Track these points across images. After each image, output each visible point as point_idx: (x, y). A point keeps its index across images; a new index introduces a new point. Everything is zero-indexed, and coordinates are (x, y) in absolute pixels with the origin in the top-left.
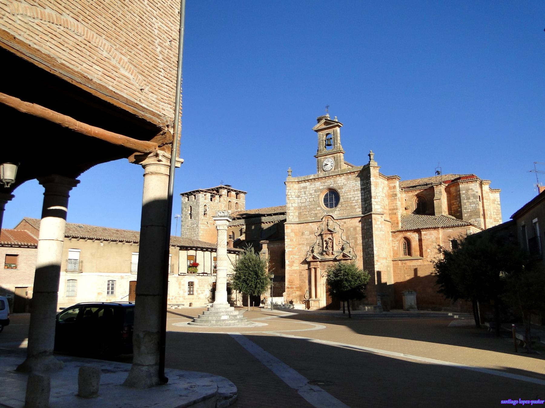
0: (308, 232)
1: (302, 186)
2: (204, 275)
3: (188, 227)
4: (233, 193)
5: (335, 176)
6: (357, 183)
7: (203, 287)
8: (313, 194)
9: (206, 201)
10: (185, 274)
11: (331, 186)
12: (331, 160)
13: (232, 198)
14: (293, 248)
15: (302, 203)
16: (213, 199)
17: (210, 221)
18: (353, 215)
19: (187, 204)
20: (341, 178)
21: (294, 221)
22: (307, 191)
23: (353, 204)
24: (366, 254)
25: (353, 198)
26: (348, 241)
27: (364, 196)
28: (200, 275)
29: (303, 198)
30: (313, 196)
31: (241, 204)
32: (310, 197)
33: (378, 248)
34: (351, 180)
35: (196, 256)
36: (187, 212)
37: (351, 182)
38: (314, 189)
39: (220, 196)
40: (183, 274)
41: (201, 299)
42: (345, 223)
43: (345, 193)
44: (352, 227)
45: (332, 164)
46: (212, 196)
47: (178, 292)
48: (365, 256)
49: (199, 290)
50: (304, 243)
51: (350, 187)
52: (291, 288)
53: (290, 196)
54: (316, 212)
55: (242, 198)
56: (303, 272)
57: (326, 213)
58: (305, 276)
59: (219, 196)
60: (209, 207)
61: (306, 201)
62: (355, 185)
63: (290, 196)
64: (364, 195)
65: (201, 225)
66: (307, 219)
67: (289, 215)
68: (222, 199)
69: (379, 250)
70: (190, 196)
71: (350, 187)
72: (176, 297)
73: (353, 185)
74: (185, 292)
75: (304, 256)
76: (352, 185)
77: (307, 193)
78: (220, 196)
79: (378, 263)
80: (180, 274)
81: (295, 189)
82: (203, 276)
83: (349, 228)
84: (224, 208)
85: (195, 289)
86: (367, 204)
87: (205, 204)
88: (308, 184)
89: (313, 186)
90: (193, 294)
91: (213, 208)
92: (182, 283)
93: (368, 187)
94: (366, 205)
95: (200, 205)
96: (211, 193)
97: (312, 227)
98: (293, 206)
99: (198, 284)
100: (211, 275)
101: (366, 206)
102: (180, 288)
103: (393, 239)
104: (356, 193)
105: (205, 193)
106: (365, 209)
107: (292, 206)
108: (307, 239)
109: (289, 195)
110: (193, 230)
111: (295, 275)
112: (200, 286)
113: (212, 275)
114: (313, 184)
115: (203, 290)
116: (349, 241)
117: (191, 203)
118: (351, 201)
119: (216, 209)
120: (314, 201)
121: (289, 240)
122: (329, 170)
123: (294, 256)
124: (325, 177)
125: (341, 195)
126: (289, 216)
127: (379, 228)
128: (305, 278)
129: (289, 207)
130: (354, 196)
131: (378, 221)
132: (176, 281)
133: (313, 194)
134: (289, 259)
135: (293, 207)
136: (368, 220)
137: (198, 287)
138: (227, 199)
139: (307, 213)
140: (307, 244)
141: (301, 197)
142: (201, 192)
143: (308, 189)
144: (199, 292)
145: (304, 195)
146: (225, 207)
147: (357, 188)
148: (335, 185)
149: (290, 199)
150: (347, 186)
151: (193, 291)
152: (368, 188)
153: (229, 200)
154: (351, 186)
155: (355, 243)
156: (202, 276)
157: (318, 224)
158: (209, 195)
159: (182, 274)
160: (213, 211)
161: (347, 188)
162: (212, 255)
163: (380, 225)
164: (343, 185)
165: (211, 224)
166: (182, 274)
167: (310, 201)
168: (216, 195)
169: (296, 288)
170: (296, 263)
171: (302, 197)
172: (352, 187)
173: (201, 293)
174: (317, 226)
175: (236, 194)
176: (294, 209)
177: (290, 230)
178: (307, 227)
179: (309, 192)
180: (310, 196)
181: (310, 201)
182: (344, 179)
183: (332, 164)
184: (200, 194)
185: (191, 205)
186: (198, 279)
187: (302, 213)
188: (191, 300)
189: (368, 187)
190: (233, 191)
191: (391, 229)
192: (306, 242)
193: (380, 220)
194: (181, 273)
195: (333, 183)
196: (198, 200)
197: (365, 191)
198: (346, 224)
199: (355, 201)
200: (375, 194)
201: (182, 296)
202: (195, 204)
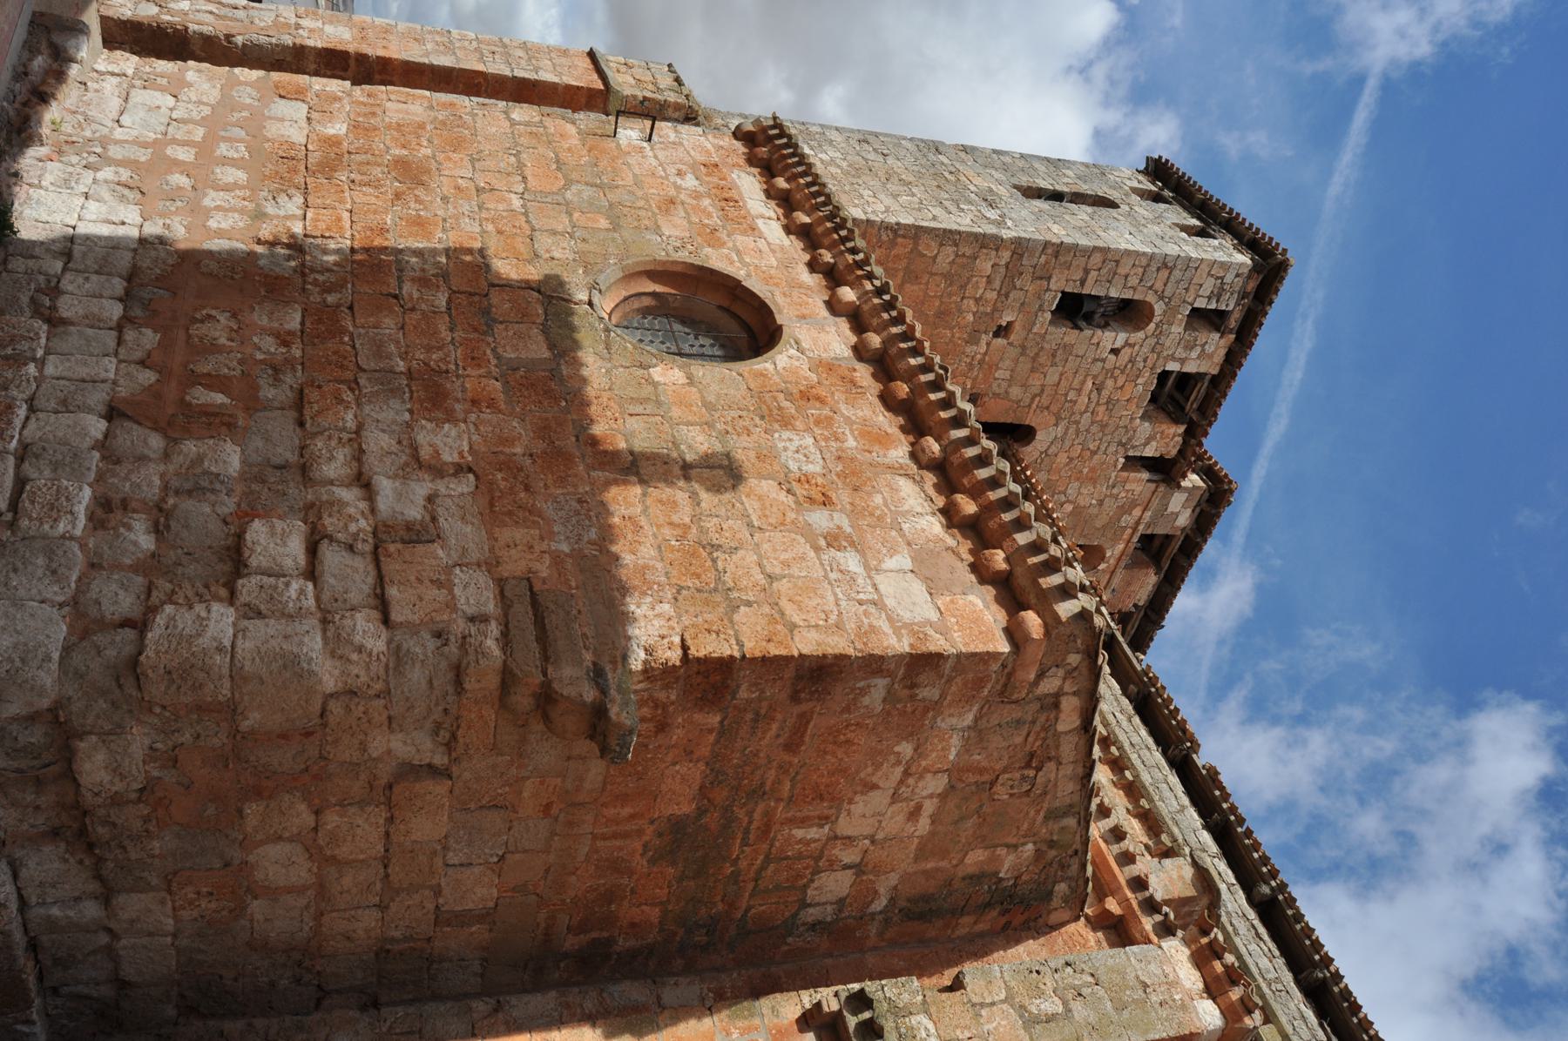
17: (1013, 352)
60: (1126, 354)
68: (1139, 489)
84: (1069, 508)
87: (1159, 308)
91: (1105, 393)
138: (1129, 531)
146: (1078, 511)
153: (1114, 552)
160: (1079, 391)
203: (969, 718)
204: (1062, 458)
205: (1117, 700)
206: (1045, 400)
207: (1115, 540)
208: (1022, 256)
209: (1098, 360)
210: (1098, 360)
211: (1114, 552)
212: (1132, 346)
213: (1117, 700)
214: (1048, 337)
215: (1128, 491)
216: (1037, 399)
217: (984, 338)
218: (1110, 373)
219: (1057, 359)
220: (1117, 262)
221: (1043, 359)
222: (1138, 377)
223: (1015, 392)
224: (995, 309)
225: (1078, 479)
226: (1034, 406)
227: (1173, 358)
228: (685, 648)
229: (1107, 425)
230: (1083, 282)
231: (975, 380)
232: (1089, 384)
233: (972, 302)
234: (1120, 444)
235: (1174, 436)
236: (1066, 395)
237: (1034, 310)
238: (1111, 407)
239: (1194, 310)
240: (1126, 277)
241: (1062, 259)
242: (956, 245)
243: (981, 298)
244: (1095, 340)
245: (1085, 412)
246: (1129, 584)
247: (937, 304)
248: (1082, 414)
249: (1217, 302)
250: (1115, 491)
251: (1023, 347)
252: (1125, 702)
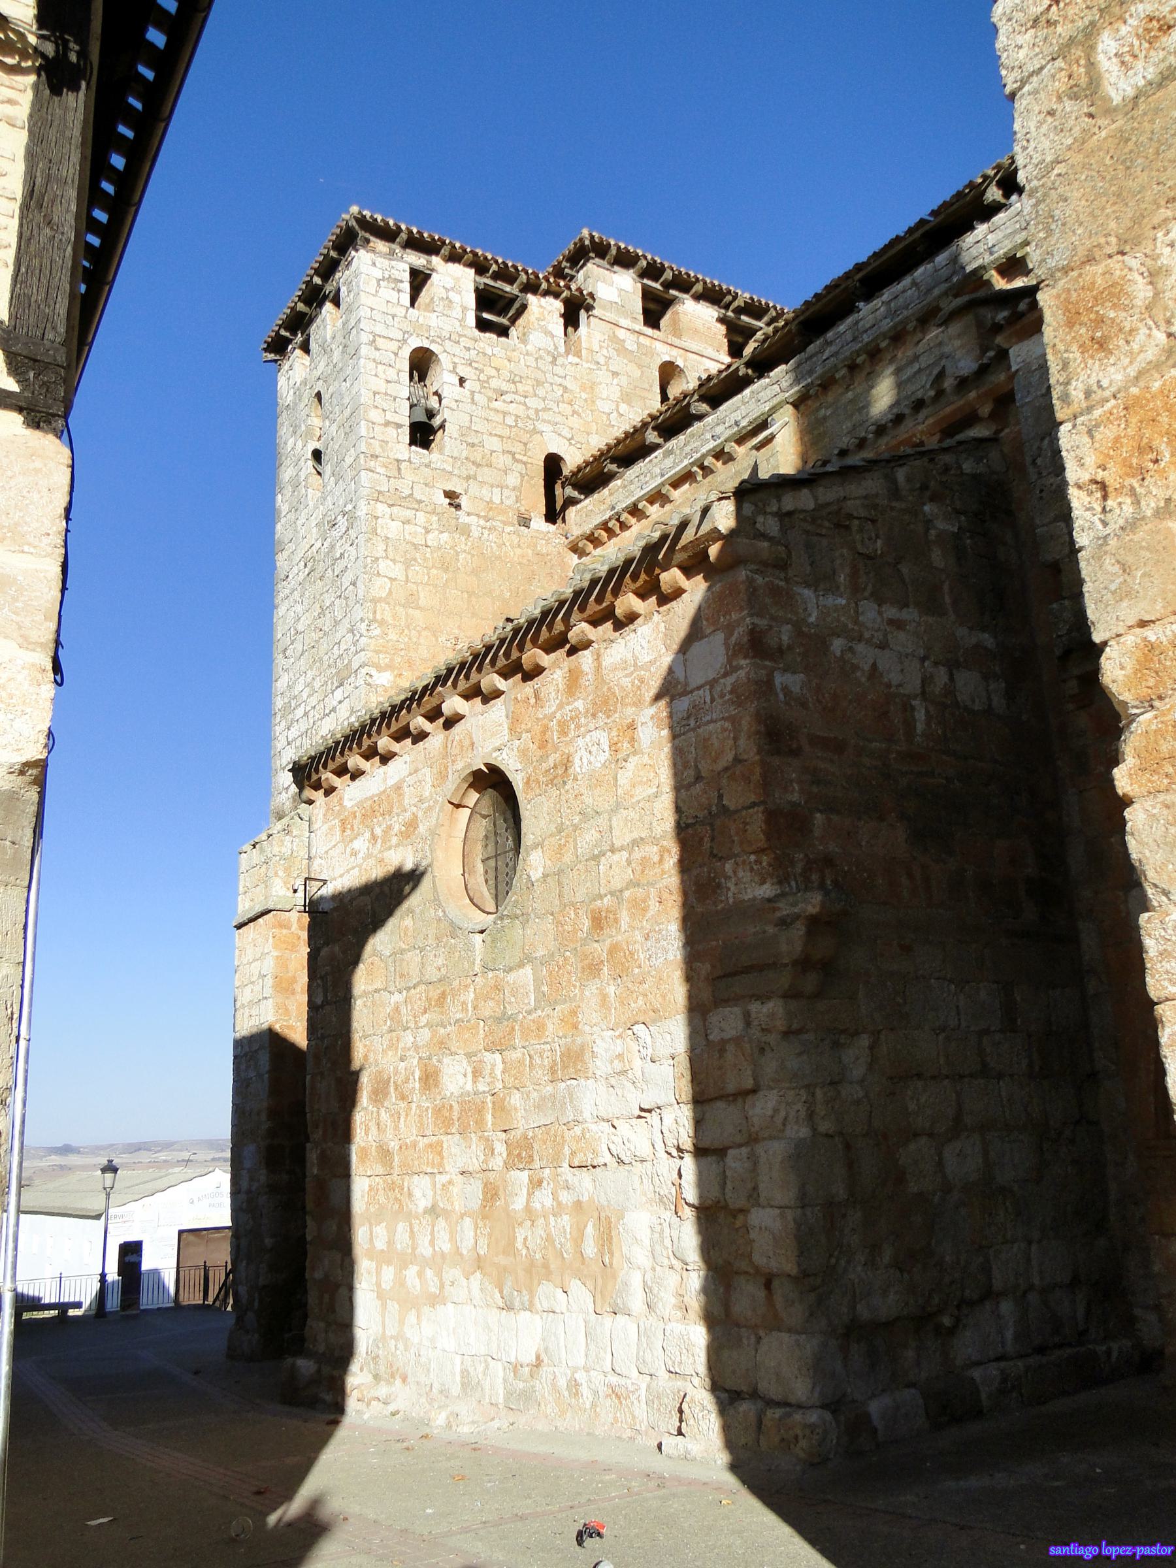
13: (694, 348)
17: (474, 488)
59: (557, 306)
60: (464, 371)
65: (381, 508)
78: (571, 319)
84: (623, 408)
91: (505, 387)
95: (365, 338)
105: (418, 260)
119: (533, 403)
138: (642, 339)
142: (381, 245)
153: (665, 354)
160: (505, 414)
165: (489, 511)
190: (697, 298)
203: (808, 593)
204: (574, 422)
205: (811, 357)
206: (518, 448)
207: (651, 353)
208: (380, 492)
209: (473, 399)
210: (473, 399)
212: (455, 365)
213: (811, 357)
214: (456, 454)
215: (601, 347)
216: (517, 456)
217: (467, 520)
218: (484, 383)
219: (476, 441)
220: (375, 393)
221: (477, 456)
222: (485, 354)
223: (513, 480)
224: (433, 512)
225: (593, 402)
226: (525, 459)
227: (462, 321)
228: (762, 851)
229: (537, 381)
230: (399, 426)
231: (505, 523)
232: (495, 405)
233: (430, 536)
234: (554, 362)
235: (541, 307)
236: (510, 427)
237: (430, 471)
238: (517, 379)
240: (388, 382)
241: (378, 451)
242: (377, 559)
243: (425, 528)
244: (454, 405)
245: (525, 404)
246: (696, 331)
247: (434, 571)
248: (528, 408)
249: (401, 281)
250: (602, 361)
251: (468, 478)
252: (811, 348)
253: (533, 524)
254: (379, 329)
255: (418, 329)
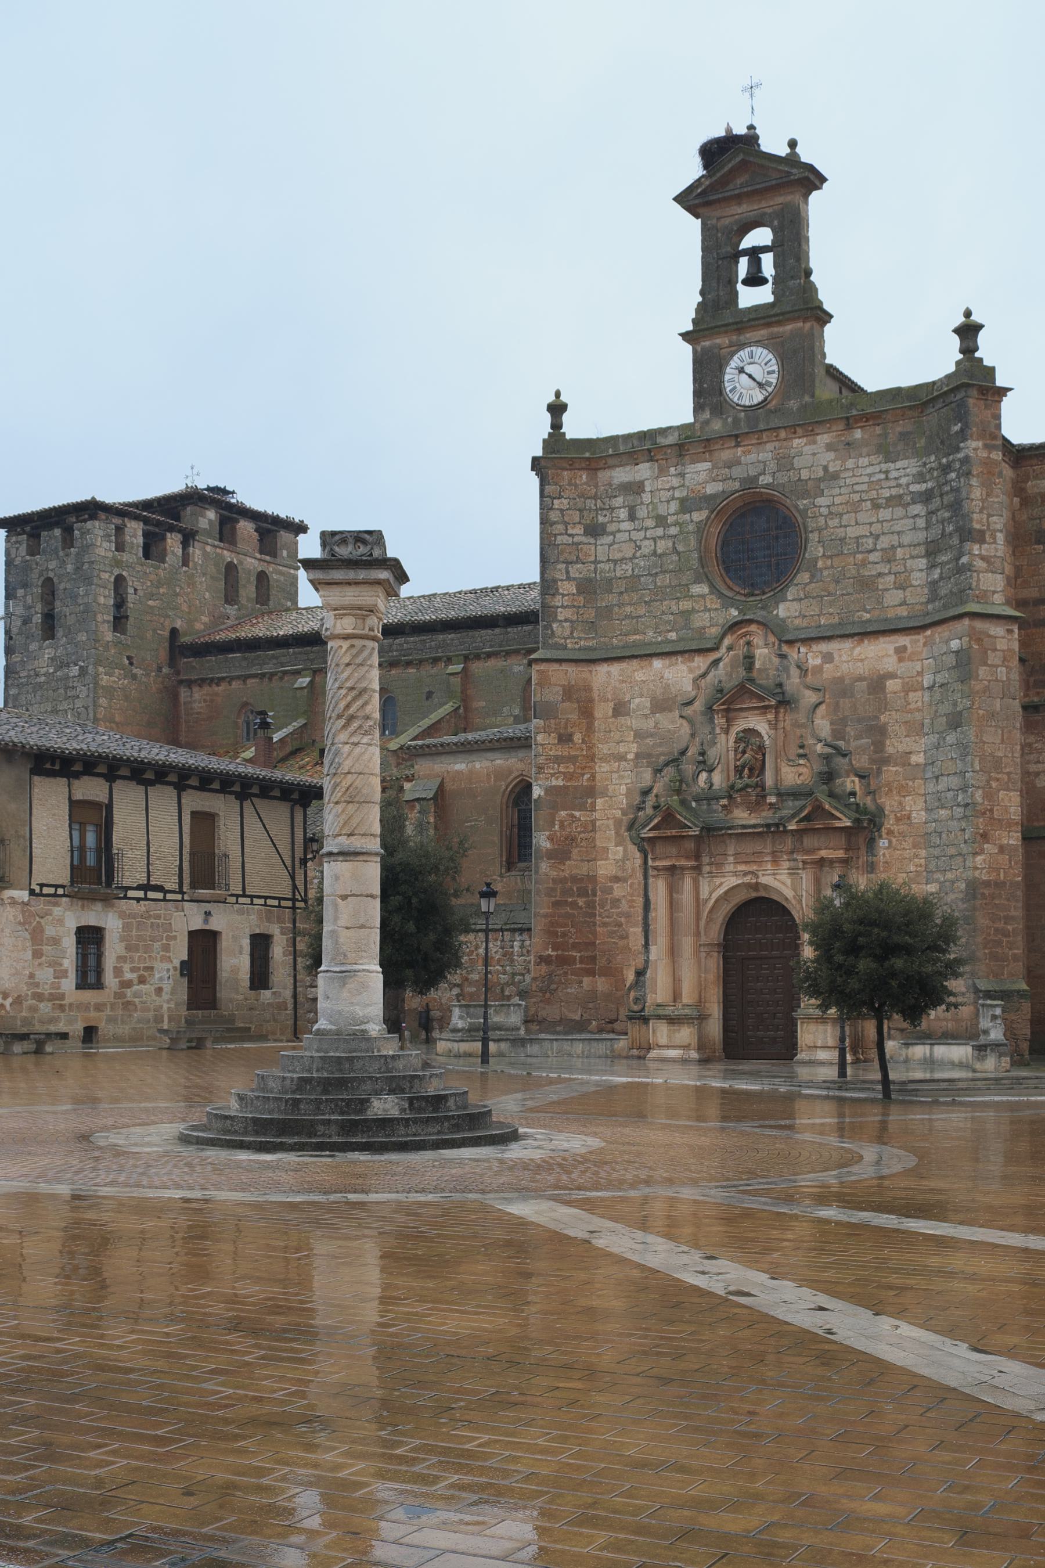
0: (647, 702)
1: (616, 481)
2: (151, 895)
3: (38, 680)
4: (246, 528)
5: (783, 434)
6: (892, 465)
7: (146, 956)
8: (670, 520)
9: (125, 557)
10: (60, 891)
11: (765, 480)
12: (765, 352)
14: (569, 777)
15: (615, 562)
16: (153, 549)
18: (869, 621)
19: (31, 569)
20: (815, 442)
21: (577, 647)
22: (642, 503)
23: (869, 572)
24: (926, 801)
25: (870, 541)
26: (841, 744)
27: (926, 529)
28: (131, 894)
29: (621, 537)
30: (673, 531)
31: (282, 579)
32: (660, 532)
33: (990, 779)
34: (865, 450)
35: (109, 807)
36: (30, 607)
37: (864, 461)
38: (677, 494)
39: (188, 537)
40: (52, 891)
41: (136, 1010)
42: (828, 658)
43: (830, 513)
44: (860, 679)
45: (769, 373)
46: (146, 535)
47: (32, 976)
48: (923, 813)
49: (126, 967)
50: (622, 750)
51: (857, 488)
52: (563, 961)
53: (560, 528)
54: (685, 605)
55: (285, 553)
56: (616, 886)
57: (734, 612)
58: (624, 906)
61: (638, 554)
62: (883, 476)
63: (560, 528)
64: (924, 525)
66: (638, 637)
67: (556, 620)
68: (197, 552)
69: (994, 784)
70: (44, 534)
71: (857, 488)
72: (19, 996)
73: (870, 475)
74: (62, 974)
75: (624, 814)
76: (866, 479)
77: (642, 512)
79: (986, 846)
80: (37, 890)
81: (582, 496)
82: (146, 899)
83: (847, 681)
85: (110, 962)
86: (938, 571)
87: (116, 572)
88: (644, 471)
89: (675, 482)
90: (99, 985)
92: (50, 931)
93: (947, 488)
94: (936, 574)
96: (146, 521)
97: (666, 676)
98: (572, 575)
99: (122, 939)
100: (179, 897)
101: (936, 576)
102: (37, 954)
103: (1031, 739)
104: (885, 514)
105: (117, 521)
106: (926, 590)
107: (568, 578)
108: (639, 735)
109: (555, 523)
110: (62, 691)
111: (581, 904)
112: (128, 948)
113: (186, 897)
114: (672, 470)
115: (146, 969)
116: (848, 742)
117: (52, 565)
118: (859, 556)
120: (678, 553)
121: (553, 738)
122: (755, 402)
123: (577, 814)
124: (737, 436)
125: (811, 524)
126: (555, 626)
127: (997, 680)
128: (628, 916)
129: (555, 581)
130: (876, 528)
131: (995, 650)
132: (20, 923)
133: (670, 520)
134: (554, 825)
135: (574, 583)
136: (947, 642)
137: (123, 953)
138: (218, 550)
139: (642, 611)
140: (638, 756)
141: (613, 534)
142: (102, 515)
143: (646, 498)
144: (128, 976)
145: (626, 526)
147: (894, 492)
148: (782, 478)
149: (560, 539)
150: (842, 483)
151: (99, 971)
152: (947, 493)
153: (228, 556)
154: (858, 480)
155: (875, 752)
156: (138, 900)
157: (695, 664)
158: (135, 532)
159: (46, 890)
161: (843, 490)
162: (183, 801)
163: (999, 669)
164: (821, 474)
166: (46, 890)
167: (659, 551)
168: (171, 529)
169: (581, 962)
170: (584, 843)
171: (619, 531)
172: (865, 487)
173: (136, 981)
174: (691, 671)
175: (256, 531)
176: (580, 591)
177: (560, 689)
178: (639, 676)
179: (655, 508)
180: (655, 527)
181: (654, 553)
182: (829, 447)
183: (769, 373)
184: (97, 523)
185: (51, 575)
186: (122, 915)
187: (616, 609)
188: (93, 1014)
189: (947, 488)
191: (1026, 695)
192: (634, 748)
193: (1002, 645)
194: (42, 885)
195: (772, 466)
196: (87, 548)
197: (932, 507)
198: (832, 662)
199: (877, 554)
200: (985, 520)
201: (51, 994)
202: (70, 568)
211: (228, 556)
217: (135, 671)
239: (117, 550)
253: (164, 670)
254: (102, 567)
255: (118, 563)
